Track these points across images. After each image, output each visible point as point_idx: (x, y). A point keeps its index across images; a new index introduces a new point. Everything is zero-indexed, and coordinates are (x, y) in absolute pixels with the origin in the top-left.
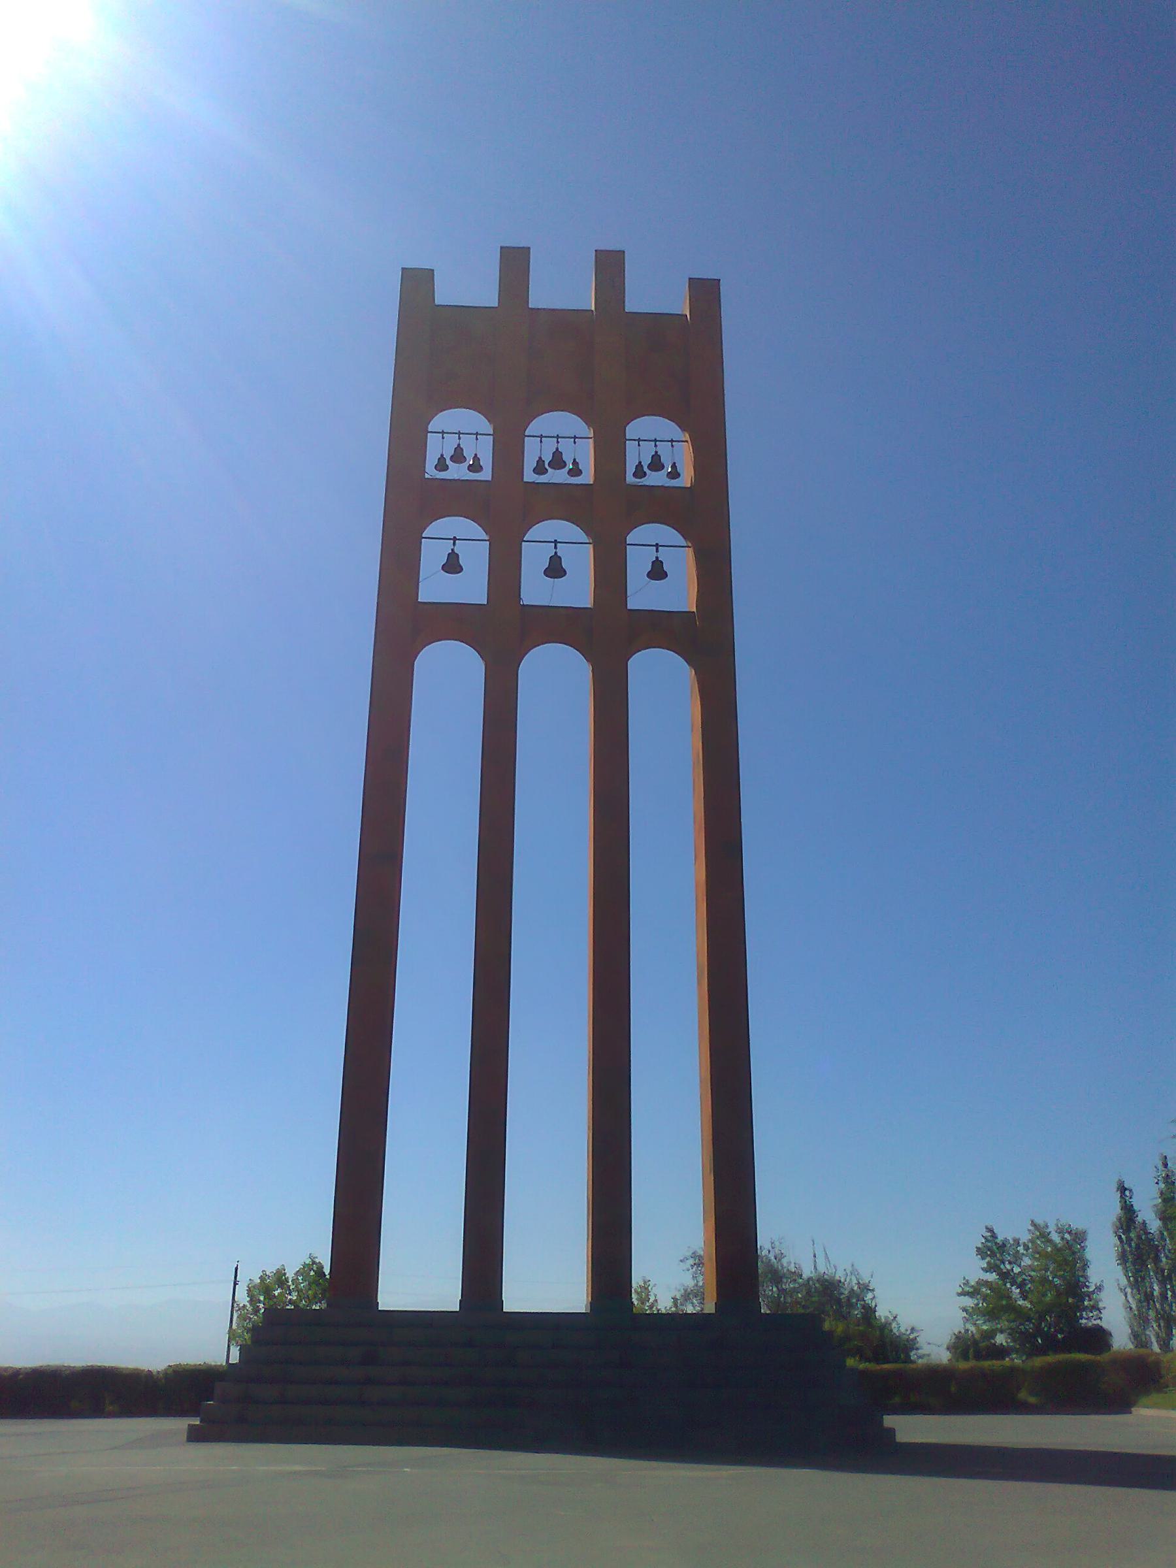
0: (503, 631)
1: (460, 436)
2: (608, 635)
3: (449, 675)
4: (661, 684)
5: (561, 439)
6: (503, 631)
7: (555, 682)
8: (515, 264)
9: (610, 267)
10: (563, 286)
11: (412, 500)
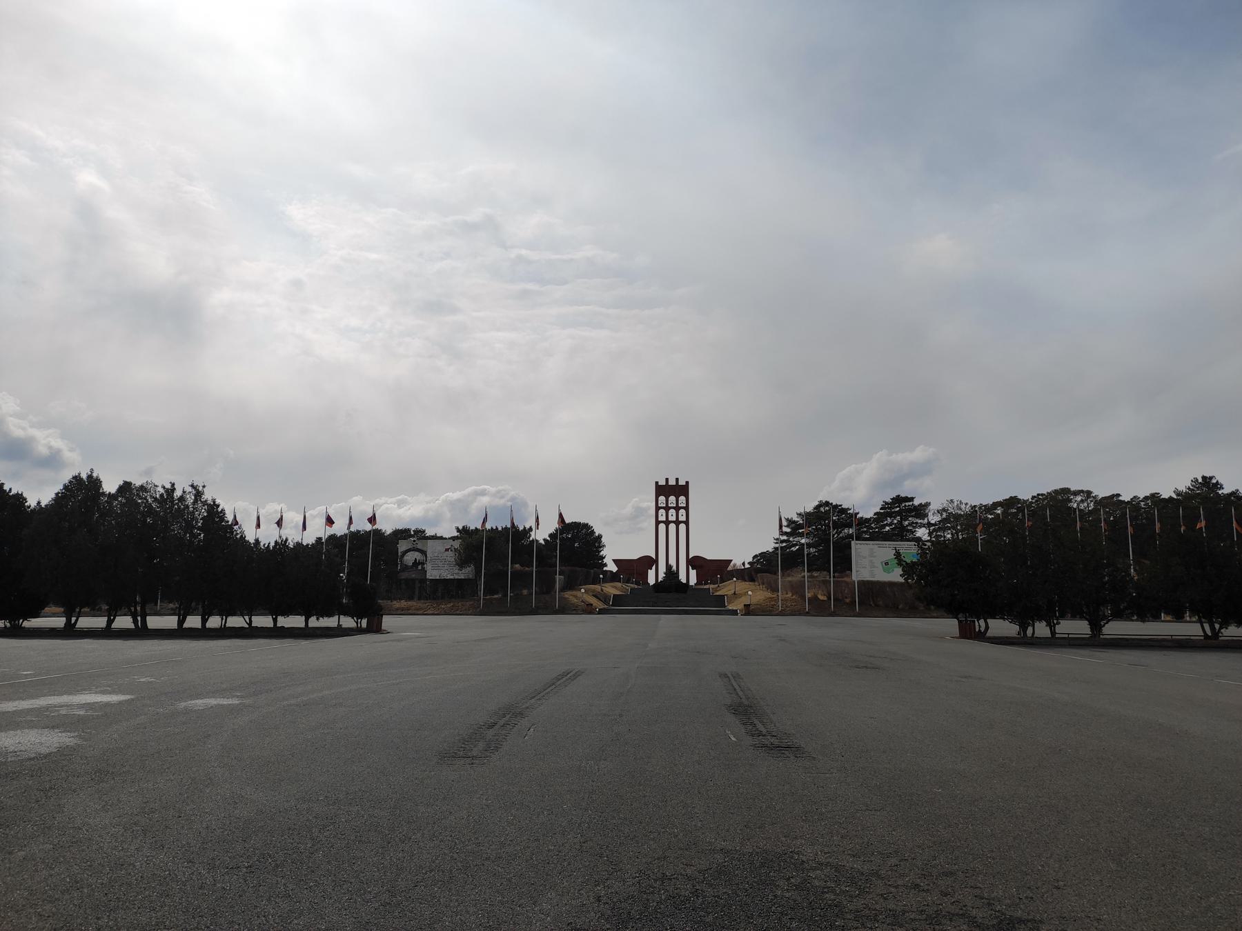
0: (667, 523)
1: (662, 499)
2: (677, 523)
3: (662, 527)
4: (682, 527)
5: (672, 499)
6: (667, 523)
7: (672, 527)
8: (667, 480)
9: (677, 480)
10: (672, 482)
11: (658, 508)
